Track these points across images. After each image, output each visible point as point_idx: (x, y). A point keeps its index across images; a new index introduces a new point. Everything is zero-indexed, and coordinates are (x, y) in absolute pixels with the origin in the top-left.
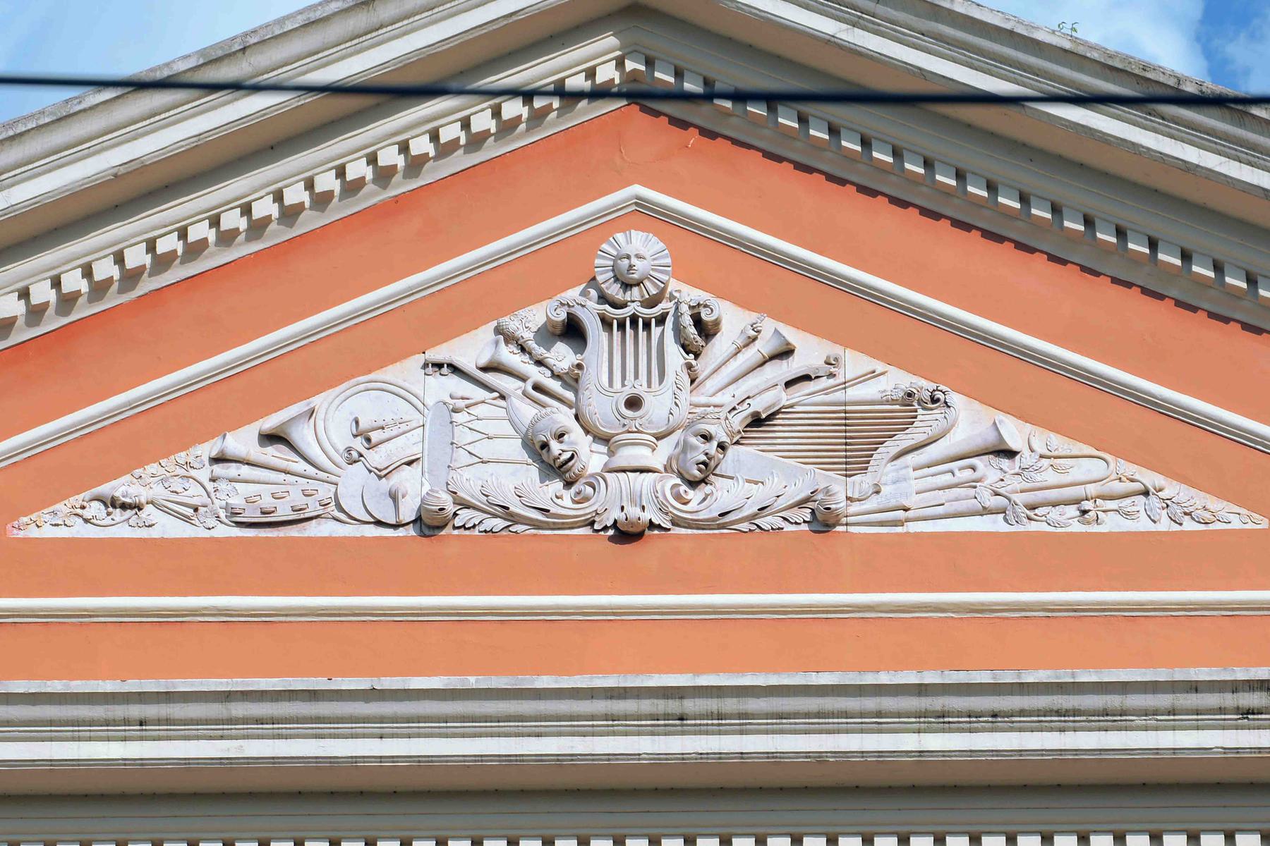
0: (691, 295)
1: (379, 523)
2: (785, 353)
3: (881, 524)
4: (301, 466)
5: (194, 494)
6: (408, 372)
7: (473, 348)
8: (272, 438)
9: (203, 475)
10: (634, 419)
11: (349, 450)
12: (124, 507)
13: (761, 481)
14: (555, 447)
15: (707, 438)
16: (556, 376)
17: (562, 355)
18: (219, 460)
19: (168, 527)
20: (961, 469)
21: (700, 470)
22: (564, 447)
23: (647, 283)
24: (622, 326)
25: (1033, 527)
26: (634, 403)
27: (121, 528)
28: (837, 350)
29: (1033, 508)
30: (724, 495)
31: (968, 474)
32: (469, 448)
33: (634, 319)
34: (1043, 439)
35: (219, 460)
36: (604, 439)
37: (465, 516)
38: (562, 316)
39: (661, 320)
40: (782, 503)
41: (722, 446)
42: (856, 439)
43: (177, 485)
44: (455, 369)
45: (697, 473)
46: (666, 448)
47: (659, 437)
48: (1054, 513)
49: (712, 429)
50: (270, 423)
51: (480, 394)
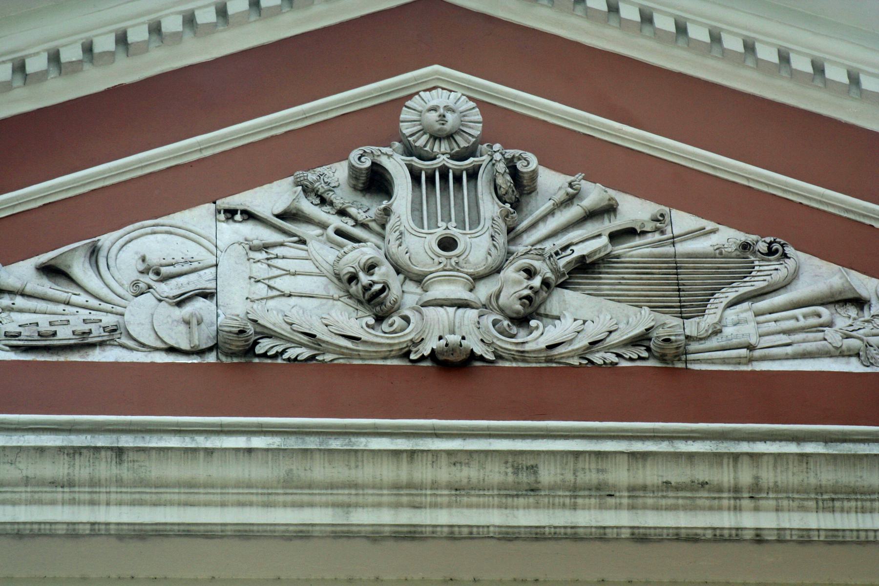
1: (172, 350)
2: (610, 209)
3: (724, 361)
4: (82, 299)
6: (199, 217)
7: (270, 198)
8: (51, 271)
10: (450, 258)
11: (135, 284)
14: (364, 279)
15: (530, 273)
16: (358, 224)
17: (367, 208)
20: (805, 316)
21: (523, 305)
22: (375, 278)
23: (458, 138)
24: (431, 180)
26: (447, 244)
32: (271, 283)
33: (444, 172)
36: (419, 279)
37: (264, 346)
38: (367, 163)
39: (473, 175)
40: (615, 338)
41: (545, 283)
44: (249, 216)
45: (518, 307)
46: (484, 291)
49: (537, 264)
51: (277, 237)
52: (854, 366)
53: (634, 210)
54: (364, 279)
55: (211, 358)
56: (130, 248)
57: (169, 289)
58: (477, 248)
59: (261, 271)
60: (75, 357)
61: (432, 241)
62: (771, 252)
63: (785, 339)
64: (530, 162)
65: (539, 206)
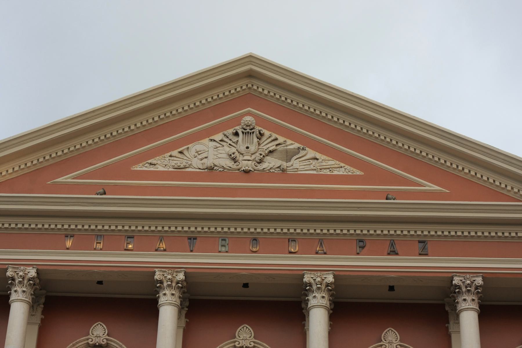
0: (258, 128)
1: (199, 169)
2: (276, 139)
4: (185, 158)
5: (166, 162)
6: (206, 141)
7: (218, 137)
8: (181, 152)
9: (167, 159)
12: (152, 164)
13: (271, 163)
14: (233, 156)
15: (261, 155)
17: (235, 139)
18: (171, 156)
19: (161, 169)
24: (246, 133)
25: (321, 173)
26: (247, 148)
27: (152, 169)
28: (286, 139)
29: (321, 169)
30: (264, 165)
31: (309, 163)
33: (248, 132)
34: (324, 157)
35: (171, 156)
37: (215, 168)
38: (235, 131)
39: (253, 133)
40: (275, 167)
41: (264, 156)
42: (289, 156)
43: (162, 161)
44: (214, 141)
46: (253, 157)
47: (252, 154)
48: (325, 171)
49: (262, 153)
50: (180, 150)
51: (218, 145)
52: (314, 172)
53: (281, 139)
54: (233, 156)
55: (206, 170)
56: (195, 147)
57: (200, 157)
58: (253, 148)
59: (216, 153)
60: (183, 170)
61: (245, 147)
62: (303, 149)
63: (304, 167)
64: (264, 131)
65: (264, 139)
